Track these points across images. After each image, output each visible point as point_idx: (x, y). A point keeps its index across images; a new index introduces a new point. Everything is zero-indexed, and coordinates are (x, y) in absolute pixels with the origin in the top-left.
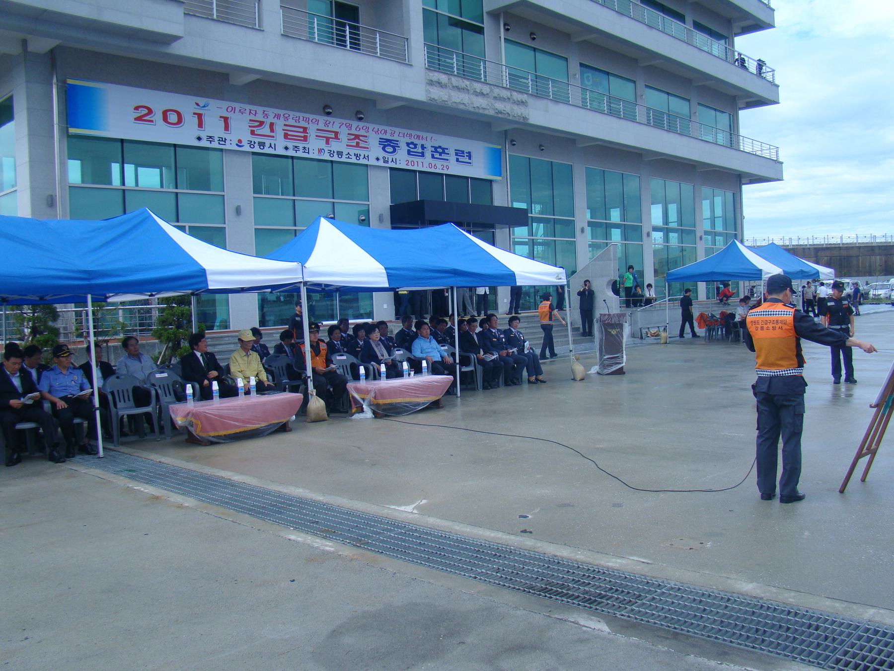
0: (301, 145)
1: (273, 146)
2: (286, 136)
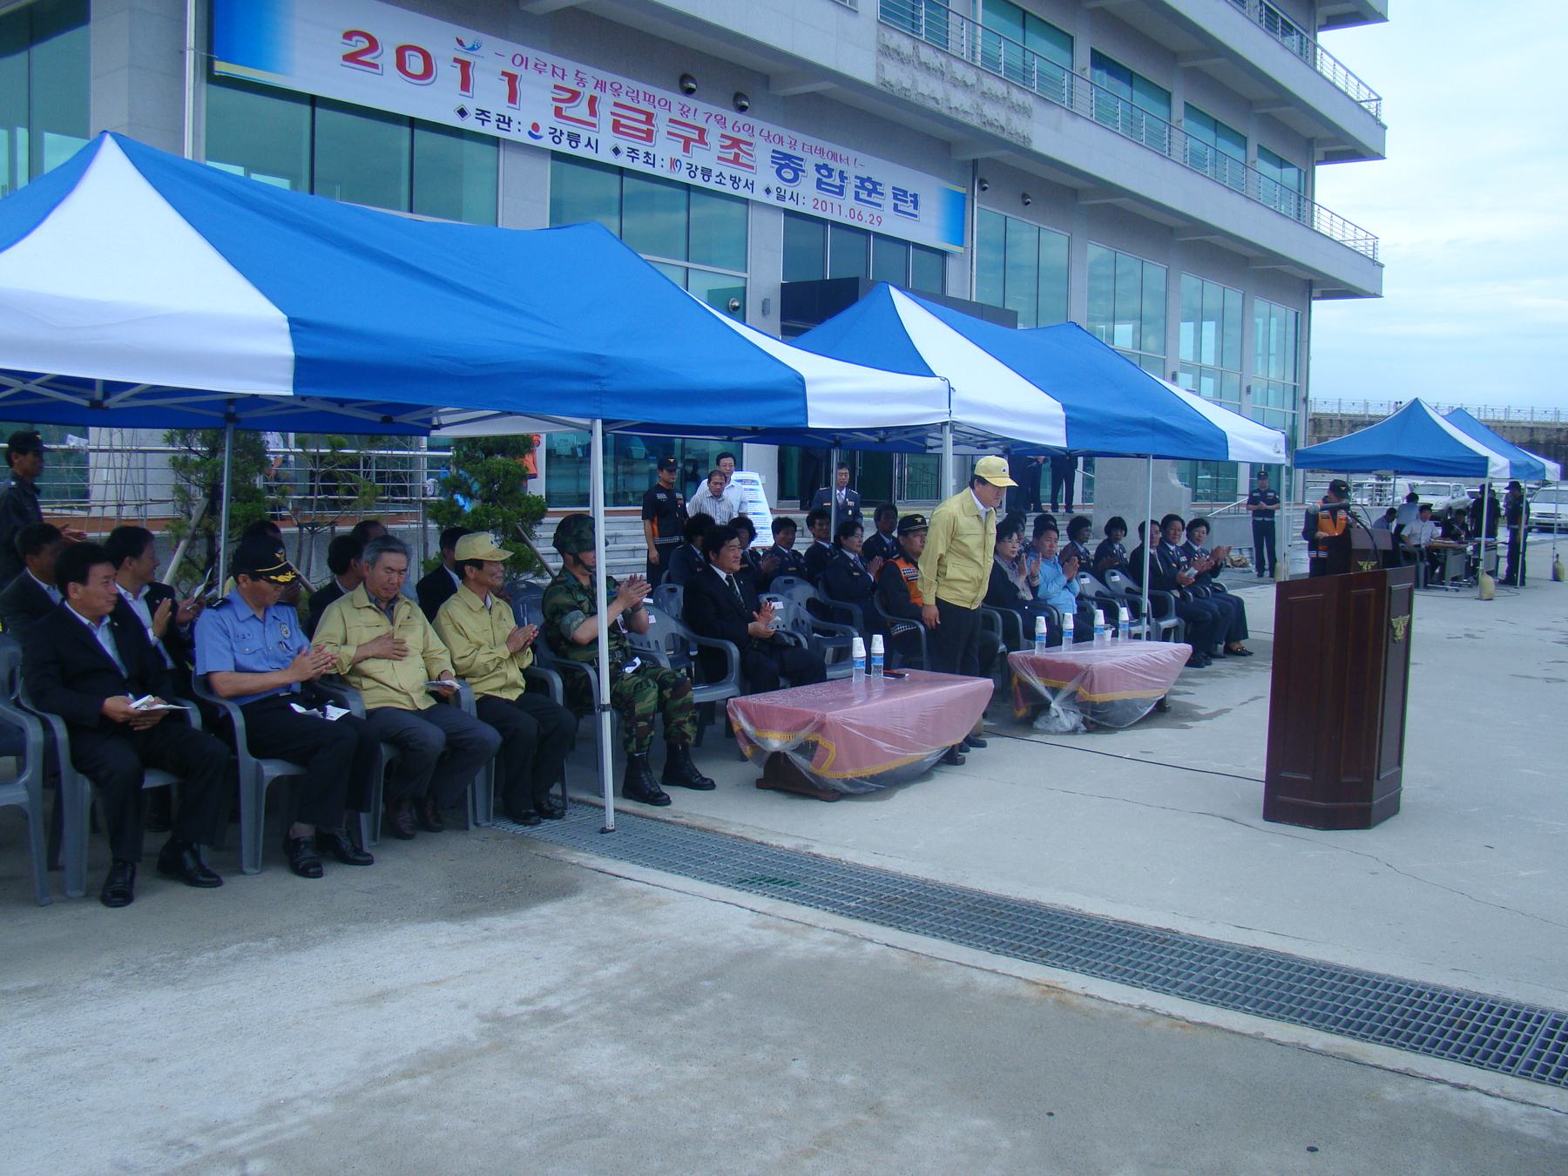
0: (643, 148)
1: (594, 144)
2: (616, 127)
